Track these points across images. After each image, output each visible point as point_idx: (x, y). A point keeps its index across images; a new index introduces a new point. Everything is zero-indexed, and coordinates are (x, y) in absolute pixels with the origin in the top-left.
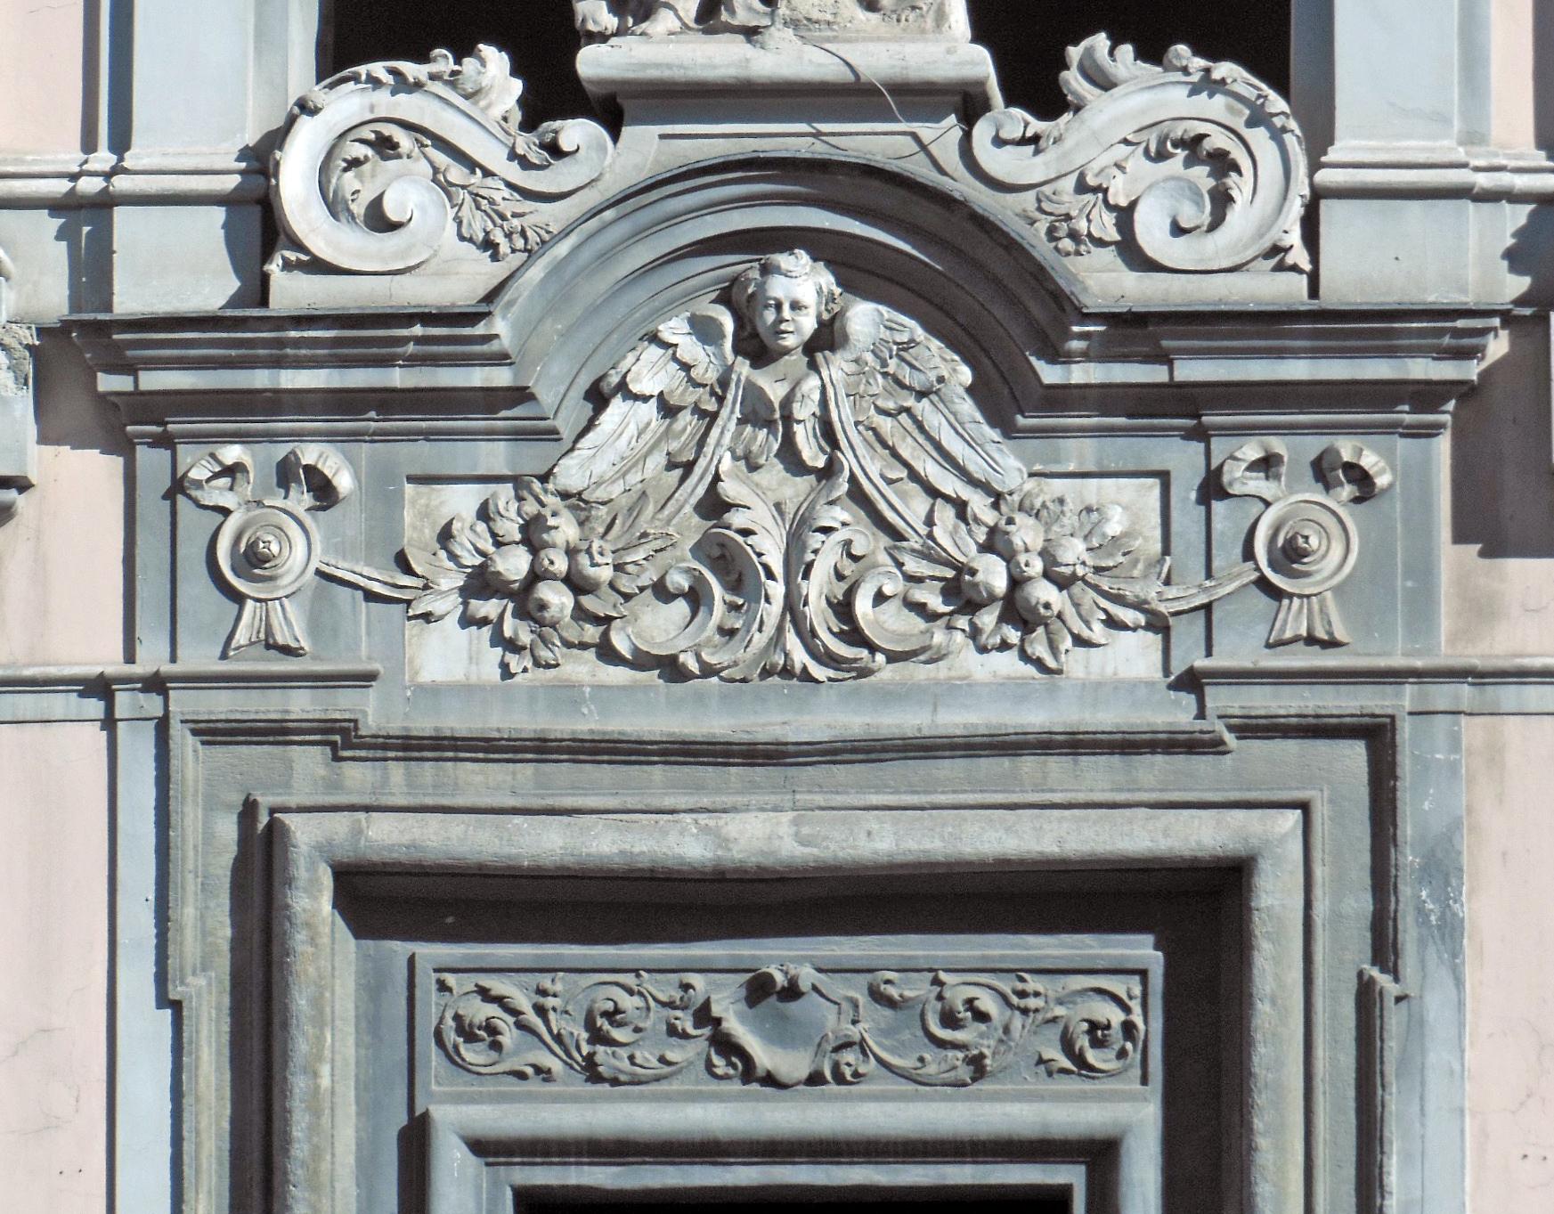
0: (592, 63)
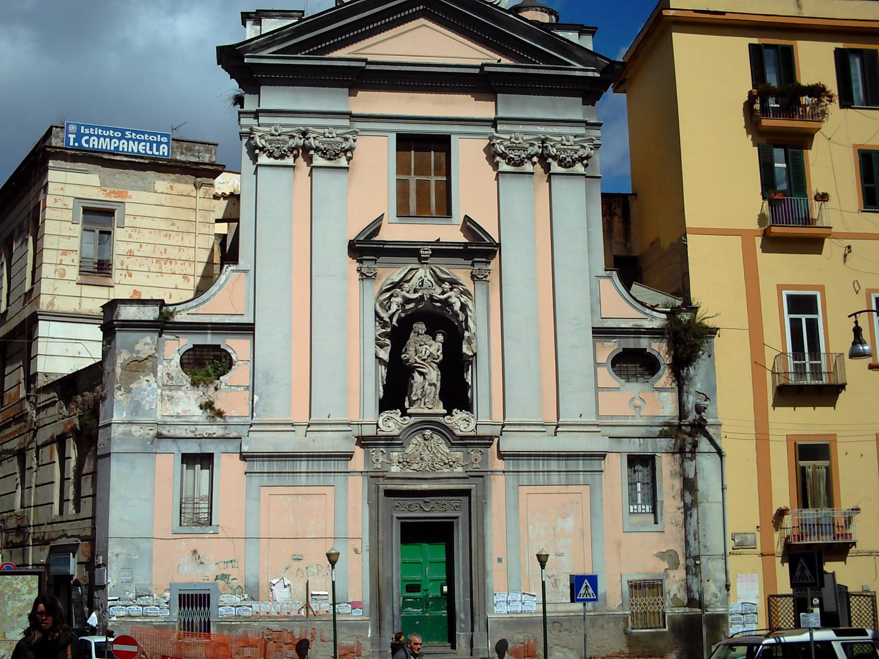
0: (408, 411)
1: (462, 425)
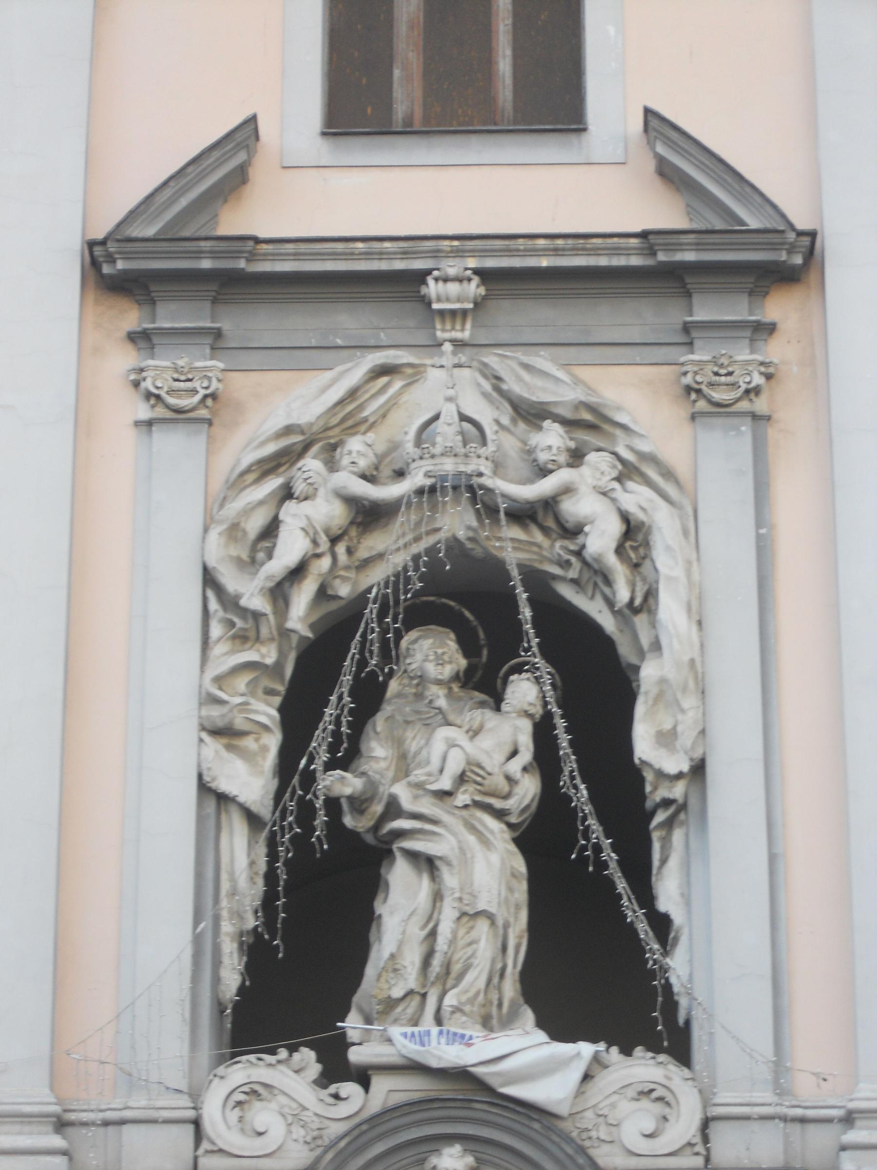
0: (356, 1055)
1: (635, 1122)
